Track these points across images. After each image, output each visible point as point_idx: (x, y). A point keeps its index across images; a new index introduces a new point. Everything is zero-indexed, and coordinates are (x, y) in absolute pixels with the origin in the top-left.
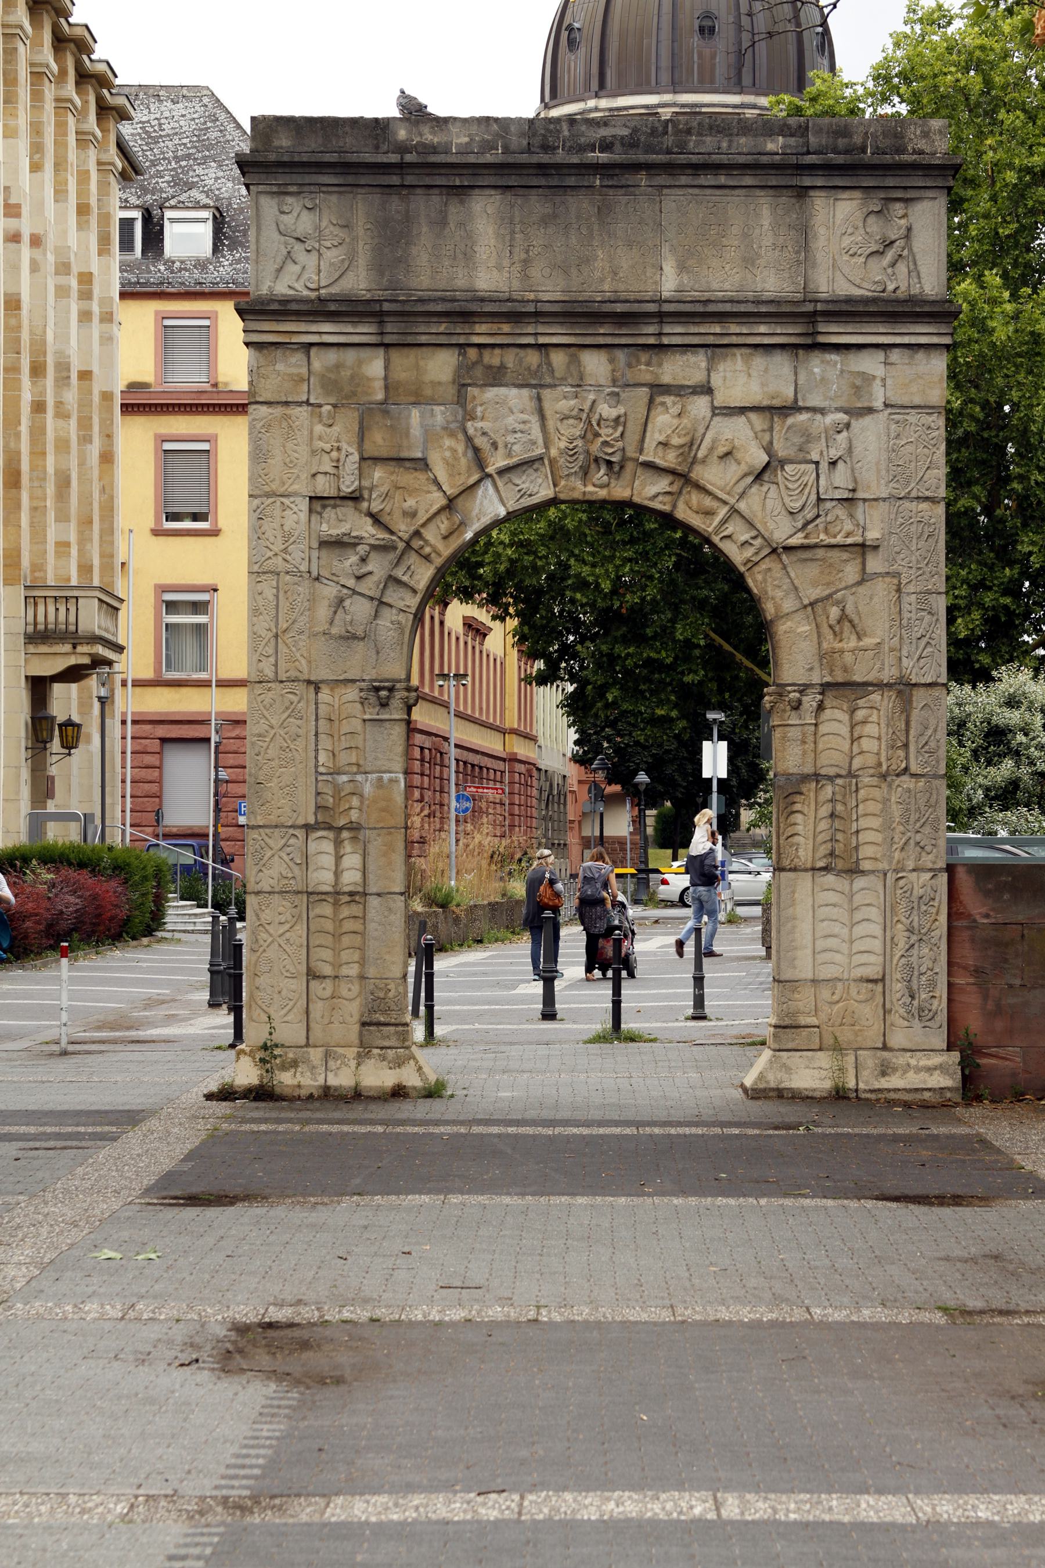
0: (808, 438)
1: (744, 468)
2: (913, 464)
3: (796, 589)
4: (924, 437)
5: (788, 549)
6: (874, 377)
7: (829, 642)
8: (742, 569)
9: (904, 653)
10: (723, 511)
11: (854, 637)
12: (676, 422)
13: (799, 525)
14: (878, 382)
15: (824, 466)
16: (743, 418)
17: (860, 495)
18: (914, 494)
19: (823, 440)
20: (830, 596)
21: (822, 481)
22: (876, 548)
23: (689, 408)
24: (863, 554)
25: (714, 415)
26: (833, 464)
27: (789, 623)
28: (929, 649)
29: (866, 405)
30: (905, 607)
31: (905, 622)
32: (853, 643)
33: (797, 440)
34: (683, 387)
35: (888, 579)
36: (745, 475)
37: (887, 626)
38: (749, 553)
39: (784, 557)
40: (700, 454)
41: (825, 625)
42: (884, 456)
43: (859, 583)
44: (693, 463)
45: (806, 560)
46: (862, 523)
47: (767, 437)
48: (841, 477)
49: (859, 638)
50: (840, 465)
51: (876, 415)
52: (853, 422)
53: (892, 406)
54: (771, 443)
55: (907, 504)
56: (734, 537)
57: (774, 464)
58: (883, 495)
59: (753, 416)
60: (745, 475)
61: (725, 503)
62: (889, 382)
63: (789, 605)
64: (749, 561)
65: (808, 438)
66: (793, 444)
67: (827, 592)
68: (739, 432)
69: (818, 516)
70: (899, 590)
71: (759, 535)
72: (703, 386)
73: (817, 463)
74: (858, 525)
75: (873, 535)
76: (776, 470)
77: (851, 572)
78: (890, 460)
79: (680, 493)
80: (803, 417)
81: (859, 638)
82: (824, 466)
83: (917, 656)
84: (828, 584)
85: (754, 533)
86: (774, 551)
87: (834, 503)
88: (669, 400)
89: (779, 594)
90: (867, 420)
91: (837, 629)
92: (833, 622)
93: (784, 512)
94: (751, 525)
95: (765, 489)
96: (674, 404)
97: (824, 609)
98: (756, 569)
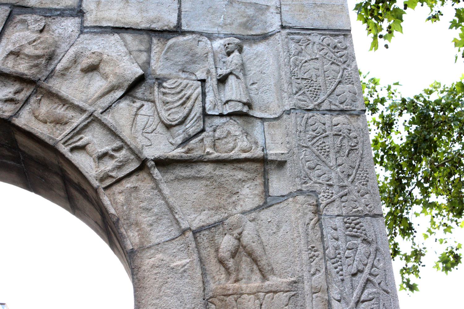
0: (194, 58)
1: (113, 80)
2: (320, 80)
3: (171, 209)
4: (331, 54)
5: (163, 163)
6: (268, 7)
7: (219, 281)
8: (96, 183)
9: (335, 293)
10: (78, 120)
11: (257, 276)
12: (34, 36)
13: (179, 140)
14: (272, 10)
15: (212, 83)
16: (117, 36)
17: (256, 113)
18: (325, 106)
19: (211, 59)
20: (221, 222)
21: (210, 98)
22: (281, 164)
23: (54, 27)
24: (265, 175)
25: (82, 32)
26: (222, 80)
27: (160, 256)
28: (370, 290)
29: (259, 32)
30: (328, 232)
31: (330, 252)
32: (256, 282)
33: (180, 59)
34: (50, 10)
35: (301, 198)
36: (112, 89)
37: (305, 256)
38: (108, 165)
39: (156, 171)
40: (59, 67)
41: (214, 261)
42: (285, 72)
43: (259, 208)
44: (48, 78)
45: (188, 178)
46: (261, 142)
47: (143, 57)
48: (233, 89)
49: (264, 278)
50: (232, 80)
51: (271, 41)
52: (245, 47)
53: (290, 28)
54: (148, 63)
55: (318, 116)
56: (89, 148)
57: (150, 81)
58: (287, 108)
59: (128, 37)
60: (112, 89)
61: (82, 110)
62: (284, 9)
63: (159, 234)
64: (107, 176)
65: (194, 58)
66: (175, 64)
67: (216, 218)
68: (111, 47)
69: (203, 131)
70: (317, 212)
71: (124, 145)
72: (73, 10)
73: (203, 81)
74: (256, 143)
75: (275, 151)
76: (151, 87)
77: (249, 195)
78: (293, 74)
79: (27, 101)
80: (189, 37)
81: (264, 278)
82: (212, 83)
83: (354, 299)
84: (217, 209)
85: (118, 143)
86: (143, 166)
87: (223, 120)
88: (30, 18)
89: (145, 219)
90: (261, 47)
91: (231, 263)
92: (224, 252)
93: (160, 129)
94: (113, 133)
95: (138, 104)
96: (36, 21)
97: (212, 240)
98: (117, 188)
